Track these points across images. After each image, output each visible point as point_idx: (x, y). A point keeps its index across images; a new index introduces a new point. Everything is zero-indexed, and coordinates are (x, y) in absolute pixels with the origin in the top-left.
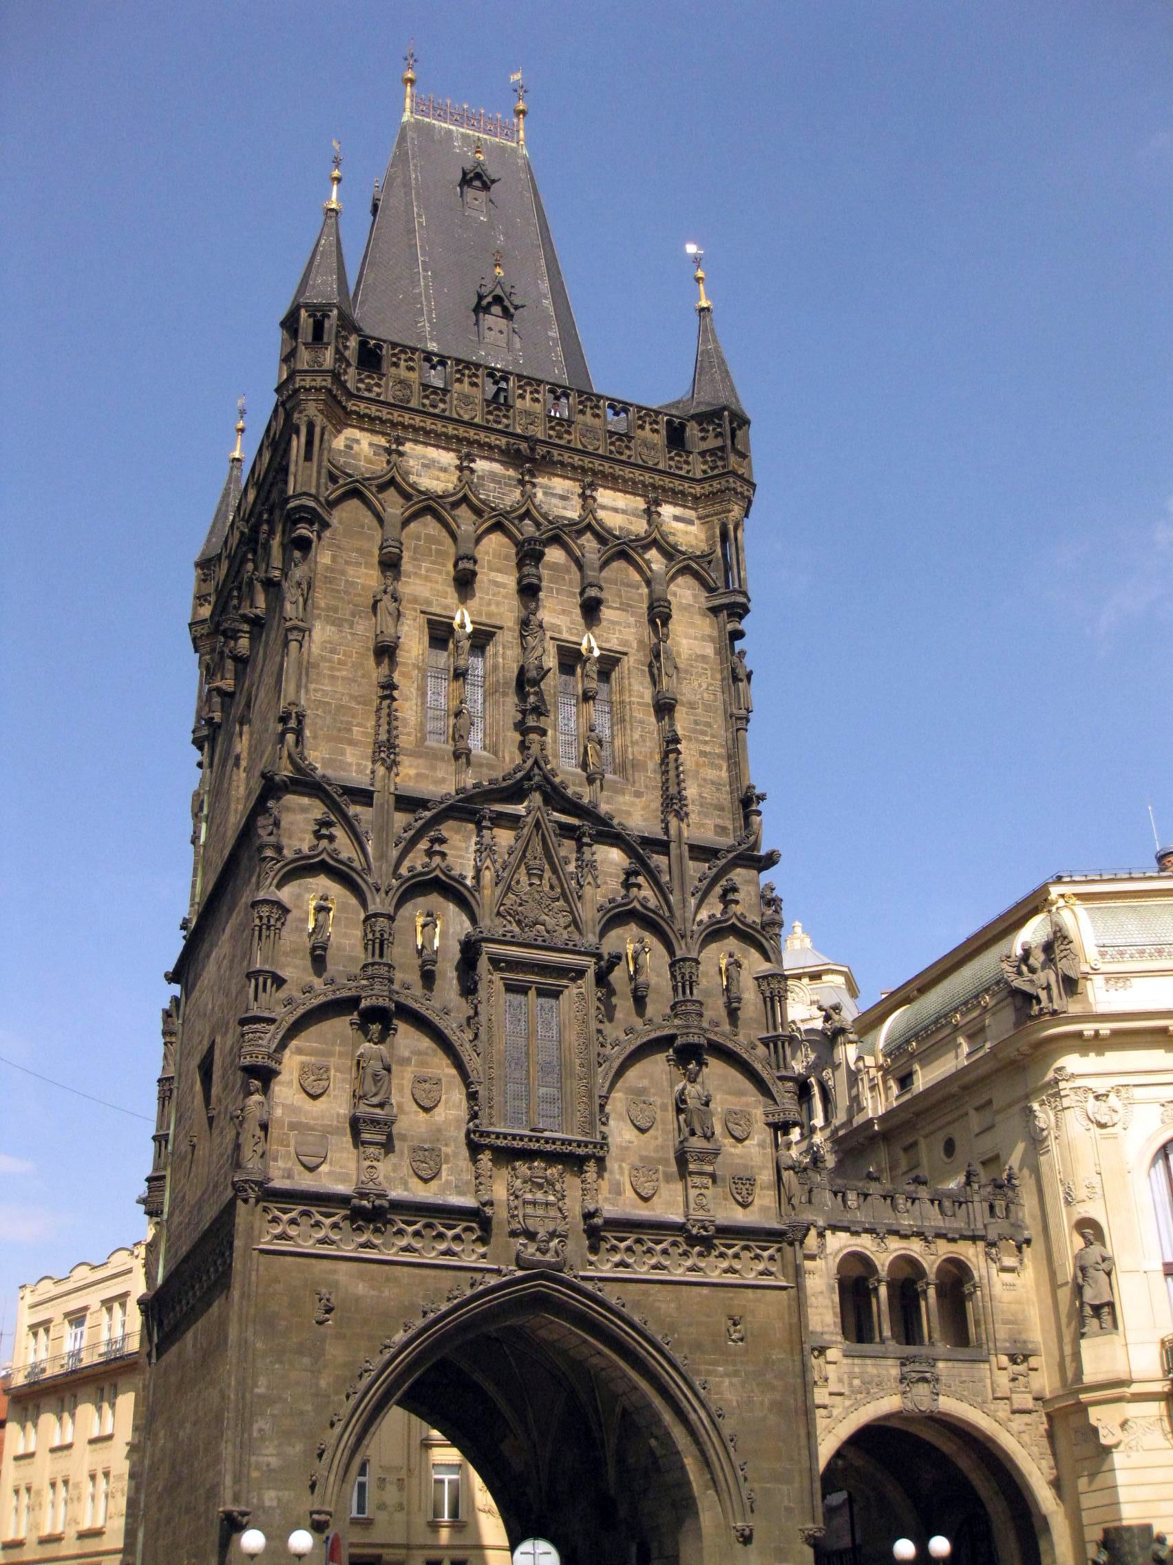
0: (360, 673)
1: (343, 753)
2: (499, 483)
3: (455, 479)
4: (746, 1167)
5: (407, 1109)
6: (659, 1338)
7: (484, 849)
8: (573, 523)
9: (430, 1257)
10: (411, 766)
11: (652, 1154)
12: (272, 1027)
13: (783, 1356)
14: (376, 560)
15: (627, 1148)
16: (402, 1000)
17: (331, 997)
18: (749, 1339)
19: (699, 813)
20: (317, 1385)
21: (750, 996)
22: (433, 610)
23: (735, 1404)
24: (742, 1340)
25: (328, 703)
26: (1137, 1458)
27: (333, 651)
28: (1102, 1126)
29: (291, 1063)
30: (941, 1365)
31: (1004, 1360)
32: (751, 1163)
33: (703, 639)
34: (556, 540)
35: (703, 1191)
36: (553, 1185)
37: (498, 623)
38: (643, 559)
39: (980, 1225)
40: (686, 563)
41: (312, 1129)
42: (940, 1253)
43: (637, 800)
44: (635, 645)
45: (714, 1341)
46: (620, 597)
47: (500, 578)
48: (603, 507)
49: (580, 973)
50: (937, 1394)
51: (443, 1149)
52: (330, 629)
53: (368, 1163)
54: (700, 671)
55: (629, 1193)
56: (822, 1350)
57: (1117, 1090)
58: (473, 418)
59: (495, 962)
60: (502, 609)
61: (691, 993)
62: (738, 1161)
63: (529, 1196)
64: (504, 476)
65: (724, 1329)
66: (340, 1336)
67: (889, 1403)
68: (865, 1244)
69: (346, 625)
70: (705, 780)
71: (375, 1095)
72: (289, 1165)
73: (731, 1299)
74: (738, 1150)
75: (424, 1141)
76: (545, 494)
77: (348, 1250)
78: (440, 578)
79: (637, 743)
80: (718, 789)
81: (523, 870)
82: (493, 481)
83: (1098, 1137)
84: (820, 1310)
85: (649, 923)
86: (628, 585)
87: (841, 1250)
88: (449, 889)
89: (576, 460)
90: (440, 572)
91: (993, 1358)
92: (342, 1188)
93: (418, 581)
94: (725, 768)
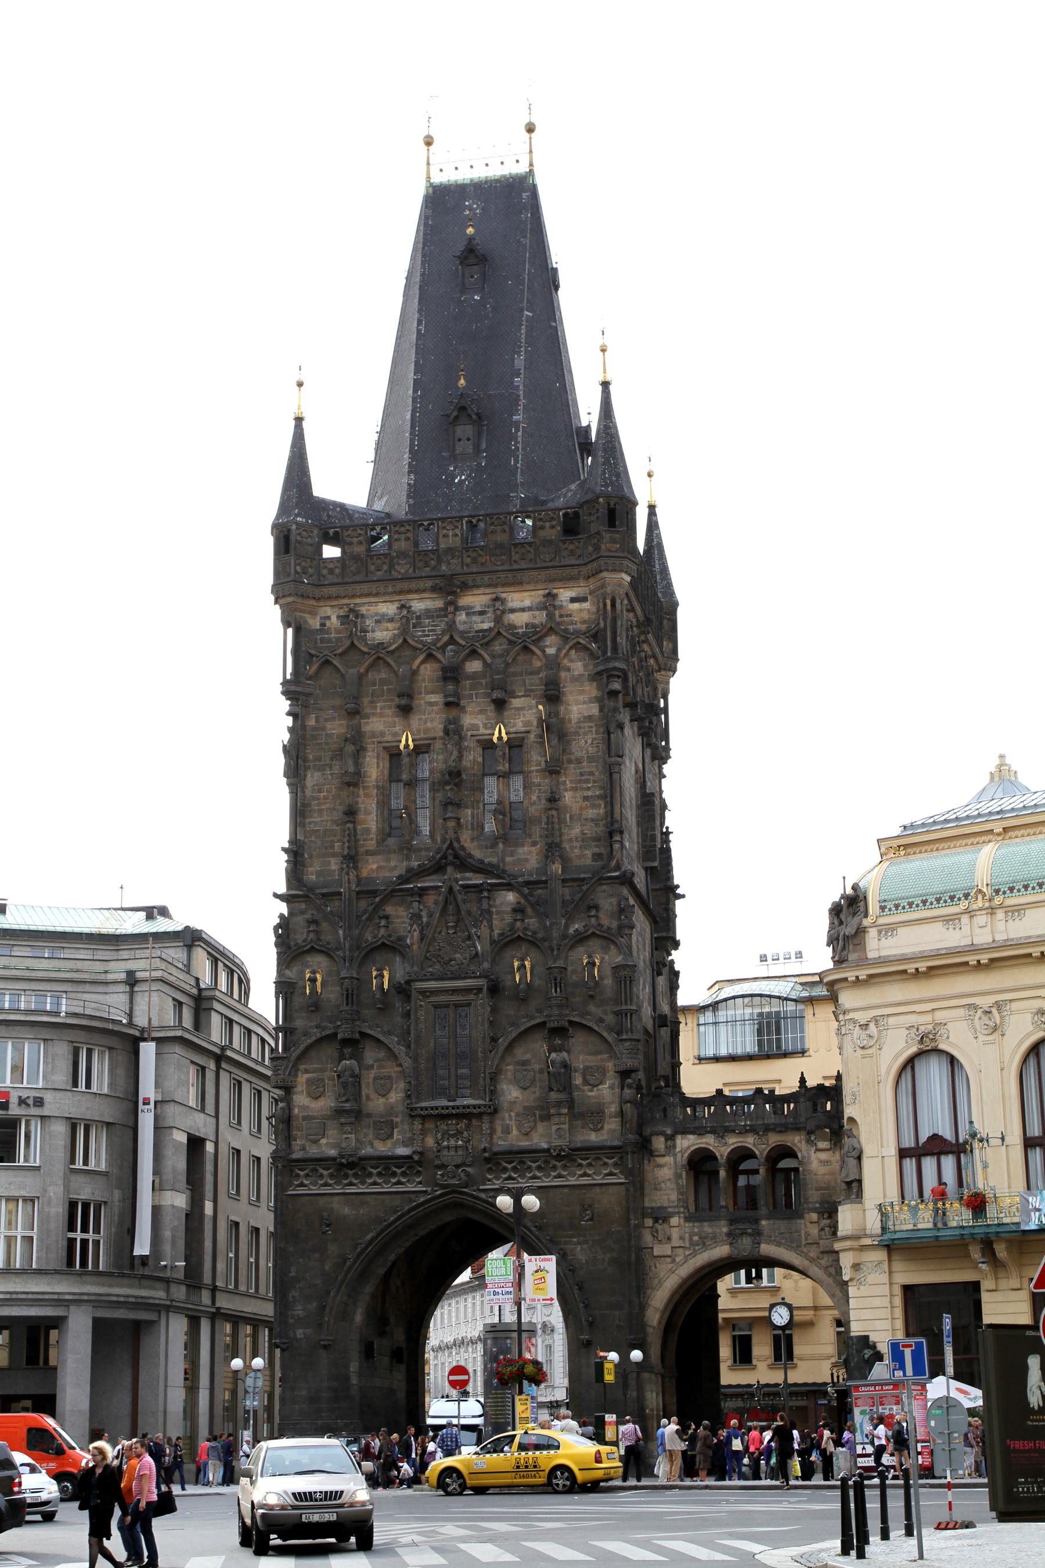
0: (338, 803)
1: (329, 864)
2: (432, 617)
5: (372, 1097)
7: (416, 917)
10: (374, 862)
11: (532, 1104)
12: (285, 1062)
13: (620, 1229)
14: (344, 712)
15: (515, 1102)
16: (363, 1030)
17: (319, 1035)
19: (580, 848)
21: (608, 982)
22: (385, 739)
23: (584, 1261)
24: (591, 1219)
25: (319, 830)
26: (864, 1290)
27: (320, 791)
28: (863, 1048)
29: (302, 1078)
30: (764, 1223)
31: (814, 1216)
33: (591, 702)
34: (473, 654)
36: (462, 1133)
38: (539, 648)
39: (803, 1119)
40: (575, 641)
41: (314, 1118)
42: (770, 1142)
43: (533, 849)
44: (535, 723)
46: (524, 685)
47: (434, 698)
48: (513, 611)
49: (479, 990)
50: (759, 1244)
51: (395, 1119)
52: (317, 774)
53: (345, 1136)
54: (587, 729)
55: (515, 1132)
56: (665, 1220)
57: (876, 1020)
59: (423, 992)
62: (594, 1101)
63: (445, 1143)
64: (436, 610)
68: (709, 1141)
69: (328, 769)
70: (586, 819)
71: (344, 1095)
75: (382, 1116)
76: (467, 614)
78: (389, 712)
79: (535, 803)
80: (596, 824)
82: (428, 617)
83: (860, 1057)
84: (667, 1192)
85: (533, 943)
87: (689, 1148)
90: (390, 707)
91: (806, 1216)
92: (333, 1152)
93: (375, 719)
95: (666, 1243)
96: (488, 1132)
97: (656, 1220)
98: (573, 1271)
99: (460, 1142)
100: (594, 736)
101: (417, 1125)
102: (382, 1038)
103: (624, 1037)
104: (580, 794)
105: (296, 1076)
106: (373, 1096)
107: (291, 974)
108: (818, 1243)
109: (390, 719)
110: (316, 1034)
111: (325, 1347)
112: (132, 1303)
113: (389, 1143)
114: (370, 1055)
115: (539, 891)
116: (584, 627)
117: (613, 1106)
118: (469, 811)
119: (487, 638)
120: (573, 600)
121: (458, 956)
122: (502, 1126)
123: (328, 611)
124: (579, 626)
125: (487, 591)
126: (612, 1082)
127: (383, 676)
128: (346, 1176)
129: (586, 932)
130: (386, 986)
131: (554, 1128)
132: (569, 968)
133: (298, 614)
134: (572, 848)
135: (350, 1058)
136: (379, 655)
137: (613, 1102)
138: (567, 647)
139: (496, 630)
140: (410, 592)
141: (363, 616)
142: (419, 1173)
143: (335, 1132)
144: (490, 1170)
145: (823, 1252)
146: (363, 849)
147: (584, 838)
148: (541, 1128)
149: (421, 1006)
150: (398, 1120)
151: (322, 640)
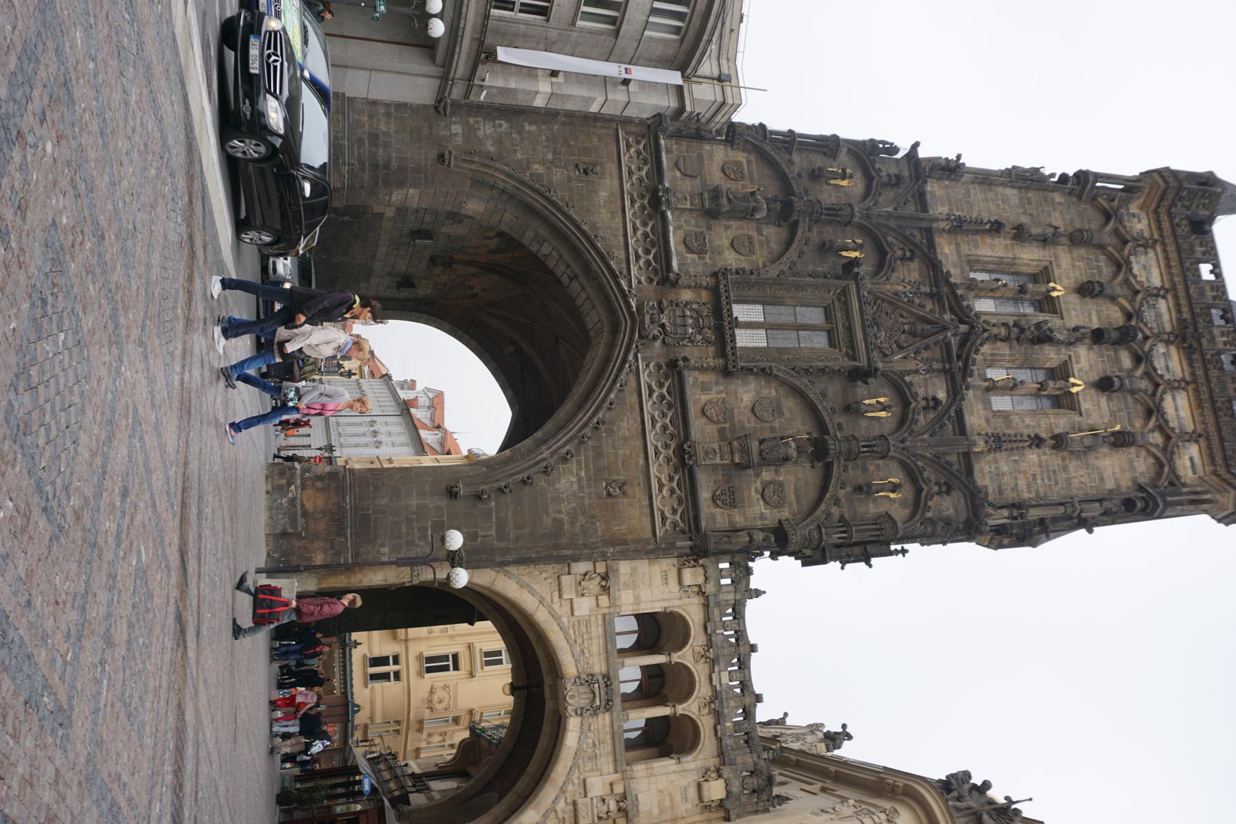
1: (943, 205)
4: (743, 502)
6: (600, 415)
9: (631, 241)
11: (736, 419)
13: (600, 533)
14: (1070, 230)
15: (736, 397)
16: (801, 225)
17: (790, 176)
18: (609, 500)
20: (535, 162)
21: (872, 509)
24: (609, 494)
27: (1003, 201)
29: (741, 157)
31: (619, 789)
32: (746, 505)
33: (1116, 480)
34: (1138, 359)
35: (718, 455)
37: (1065, 317)
40: (1165, 462)
43: (983, 420)
44: (1090, 422)
45: (604, 469)
47: (1094, 318)
50: (581, 715)
51: (707, 257)
53: (688, 198)
55: (704, 398)
56: (606, 589)
59: (845, 292)
60: (1075, 319)
61: (864, 446)
62: (746, 495)
63: (688, 313)
65: (615, 477)
66: (569, 179)
67: (569, 667)
68: (697, 638)
70: (1016, 478)
71: (735, 197)
72: (675, 152)
73: (639, 485)
74: (755, 495)
76: (1164, 354)
77: (627, 186)
78: (1077, 275)
79: (1023, 422)
80: (1013, 489)
81: (912, 320)
82: (1156, 316)
85: (903, 420)
86: (1129, 419)
88: (883, 263)
89: (1200, 373)
90: (1081, 275)
93: (1069, 259)
94: (1030, 496)
95: (577, 592)
96: (705, 365)
97: (605, 577)
98: (545, 472)
99: (690, 331)
100: (1088, 485)
101: (707, 281)
102: (794, 246)
103: (823, 531)
104: (1038, 470)
105: (743, 151)
106: (731, 233)
107: (843, 157)
108: (585, 796)
109: (1072, 275)
110: (792, 172)
111: (441, 157)
112: (459, 23)
113: (682, 248)
114: (774, 234)
115: (950, 427)
117: (742, 520)
120: (1191, 459)
121: (883, 333)
122: (709, 383)
123: (1145, 222)
126: (768, 516)
127: (1105, 270)
128: (642, 197)
129: (924, 481)
130: (844, 254)
131: (716, 447)
132: (881, 462)
133: (1146, 191)
134: (989, 462)
135: (769, 210)
136: (1121, 265)
137: (745, 518)
138: (1159, 454)
139: (1161, 382)
141: (1146, 253)
142: (651, 281)
143: (689, 189)
144: (659, 367)
145: (575, 803)
146: (960, 240)
147: (1000, 475)
148: (711, 429)
149: (829, 291)
150: (707, 260)
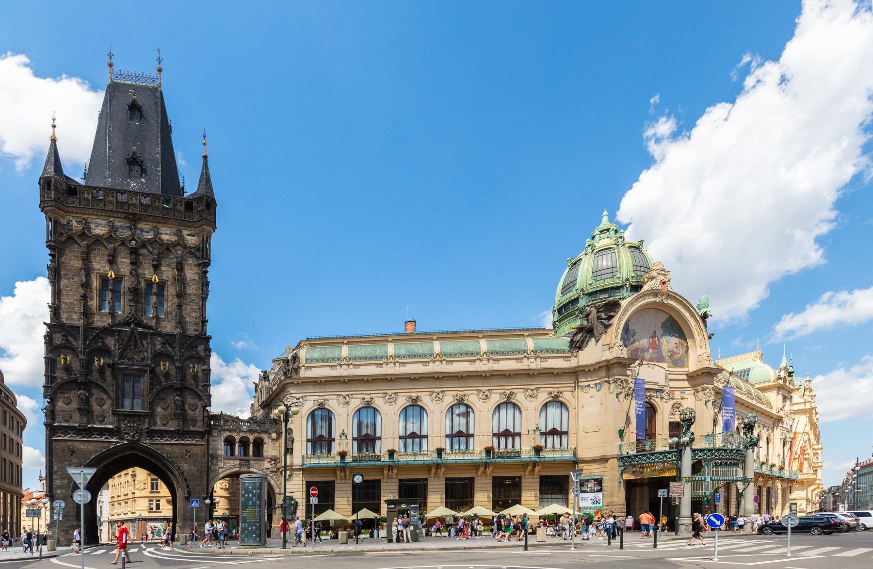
3: (107, 229)
8: (149, 240)
58: (112, 208)
60: (125, 270)
76: (141, 231)
90: (103, 260)
116: (194, 246)
118: (141, 305)
119: (152, 242)
123: (71, 218)
124: (191, 245)
125: (150, 224)
140: (113, 217)
141: (89, 223)
151: (68, 229)
